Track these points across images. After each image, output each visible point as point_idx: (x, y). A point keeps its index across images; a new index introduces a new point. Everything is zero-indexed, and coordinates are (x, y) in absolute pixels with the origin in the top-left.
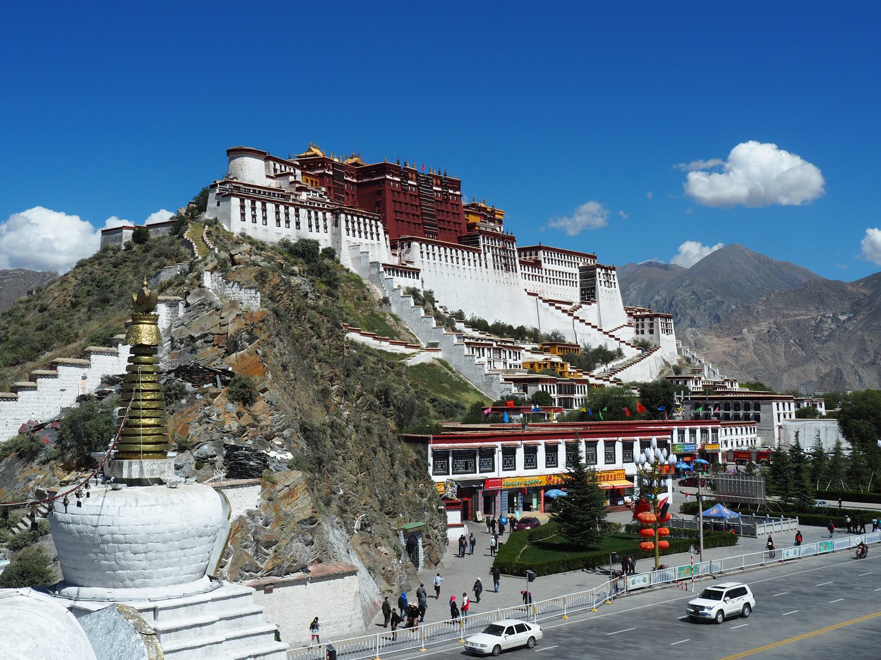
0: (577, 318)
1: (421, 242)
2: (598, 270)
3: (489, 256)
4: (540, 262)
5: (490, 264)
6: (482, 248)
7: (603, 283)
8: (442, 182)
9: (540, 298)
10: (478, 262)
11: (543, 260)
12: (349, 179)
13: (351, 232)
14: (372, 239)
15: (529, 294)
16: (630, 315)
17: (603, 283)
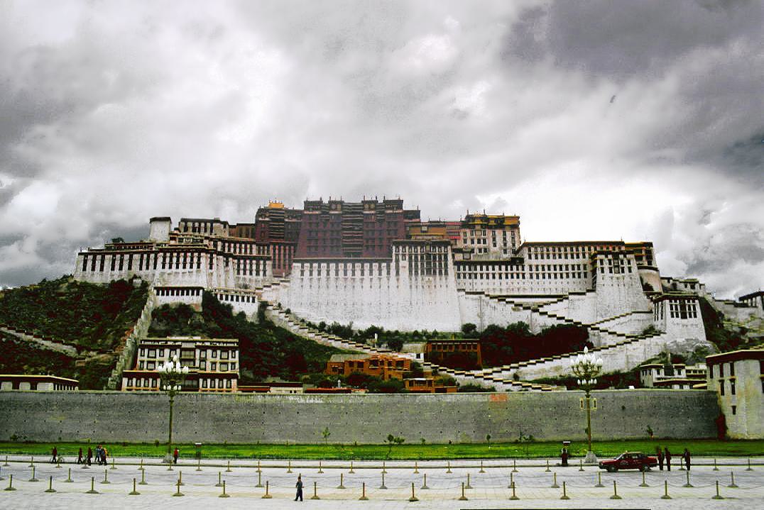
0: (537, 311)
1: (303, 262)
2: (599, 257)
3: (404, 263)
4: (522, 261)
5: (404, 273)
6: (394, 258)
7: (607, 270)
8: (376, 206)
9: (487, 296)
10: (384, 272)
11: (526, 257)
12: (294, 220)
13: (167, 266)
14: (191, 267)
15: (467, 293)
16: (652, 300)
17: (607, 270)
